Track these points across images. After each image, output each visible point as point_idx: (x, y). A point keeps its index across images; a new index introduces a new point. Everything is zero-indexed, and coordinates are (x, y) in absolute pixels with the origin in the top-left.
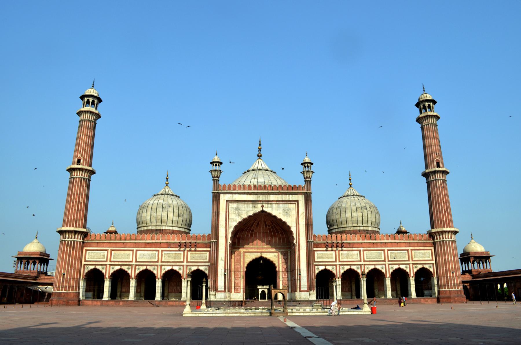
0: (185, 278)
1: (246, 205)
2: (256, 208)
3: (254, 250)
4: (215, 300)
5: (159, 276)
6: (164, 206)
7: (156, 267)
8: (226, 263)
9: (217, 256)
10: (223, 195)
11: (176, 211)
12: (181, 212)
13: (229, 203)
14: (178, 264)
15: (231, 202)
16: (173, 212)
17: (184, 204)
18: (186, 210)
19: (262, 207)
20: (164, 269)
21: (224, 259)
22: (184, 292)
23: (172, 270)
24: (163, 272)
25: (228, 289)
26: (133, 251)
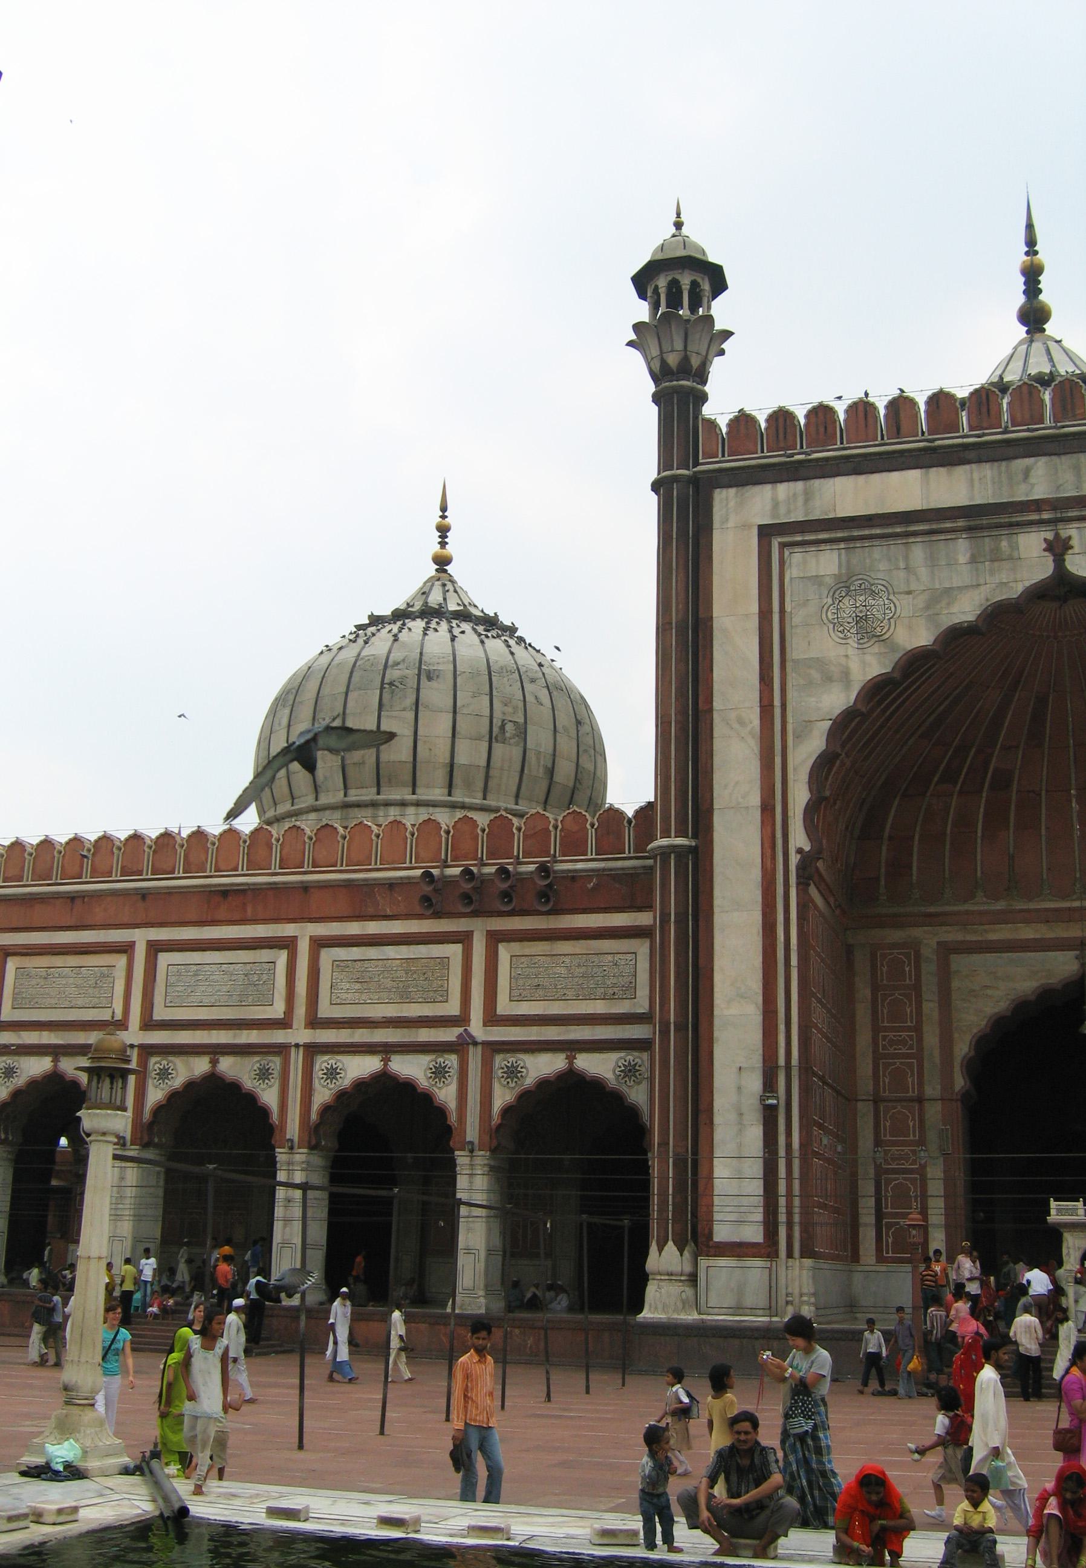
0: (471, 1143)
1: (918, 552)
2: (1006, 565)
3: (1028, 932)
4: (691, 1317)
5: (293, 1128)
6: (392, 674)
7: (275, 1062)
8: (776, 1012)
9: (702, 962)
10: (732, 491)
11: (475, 705)
12: (510, 710)
13: (783, 546)
14: (425, 1035)
15: (798, 538)
16: (455, 712)
17: (540, 665)
18: (546, 701)
19: (1058, 549)
20: (332, 1073)
21: (755, 984)
22: (468, 1250)
23: (384, 1081)
24: (323, 1095)
25: (797, 1230)
26: (127, 949)
